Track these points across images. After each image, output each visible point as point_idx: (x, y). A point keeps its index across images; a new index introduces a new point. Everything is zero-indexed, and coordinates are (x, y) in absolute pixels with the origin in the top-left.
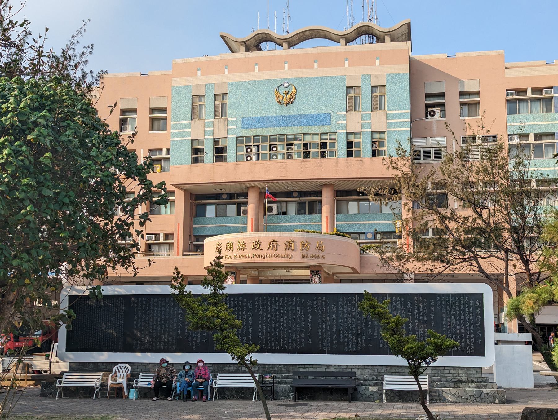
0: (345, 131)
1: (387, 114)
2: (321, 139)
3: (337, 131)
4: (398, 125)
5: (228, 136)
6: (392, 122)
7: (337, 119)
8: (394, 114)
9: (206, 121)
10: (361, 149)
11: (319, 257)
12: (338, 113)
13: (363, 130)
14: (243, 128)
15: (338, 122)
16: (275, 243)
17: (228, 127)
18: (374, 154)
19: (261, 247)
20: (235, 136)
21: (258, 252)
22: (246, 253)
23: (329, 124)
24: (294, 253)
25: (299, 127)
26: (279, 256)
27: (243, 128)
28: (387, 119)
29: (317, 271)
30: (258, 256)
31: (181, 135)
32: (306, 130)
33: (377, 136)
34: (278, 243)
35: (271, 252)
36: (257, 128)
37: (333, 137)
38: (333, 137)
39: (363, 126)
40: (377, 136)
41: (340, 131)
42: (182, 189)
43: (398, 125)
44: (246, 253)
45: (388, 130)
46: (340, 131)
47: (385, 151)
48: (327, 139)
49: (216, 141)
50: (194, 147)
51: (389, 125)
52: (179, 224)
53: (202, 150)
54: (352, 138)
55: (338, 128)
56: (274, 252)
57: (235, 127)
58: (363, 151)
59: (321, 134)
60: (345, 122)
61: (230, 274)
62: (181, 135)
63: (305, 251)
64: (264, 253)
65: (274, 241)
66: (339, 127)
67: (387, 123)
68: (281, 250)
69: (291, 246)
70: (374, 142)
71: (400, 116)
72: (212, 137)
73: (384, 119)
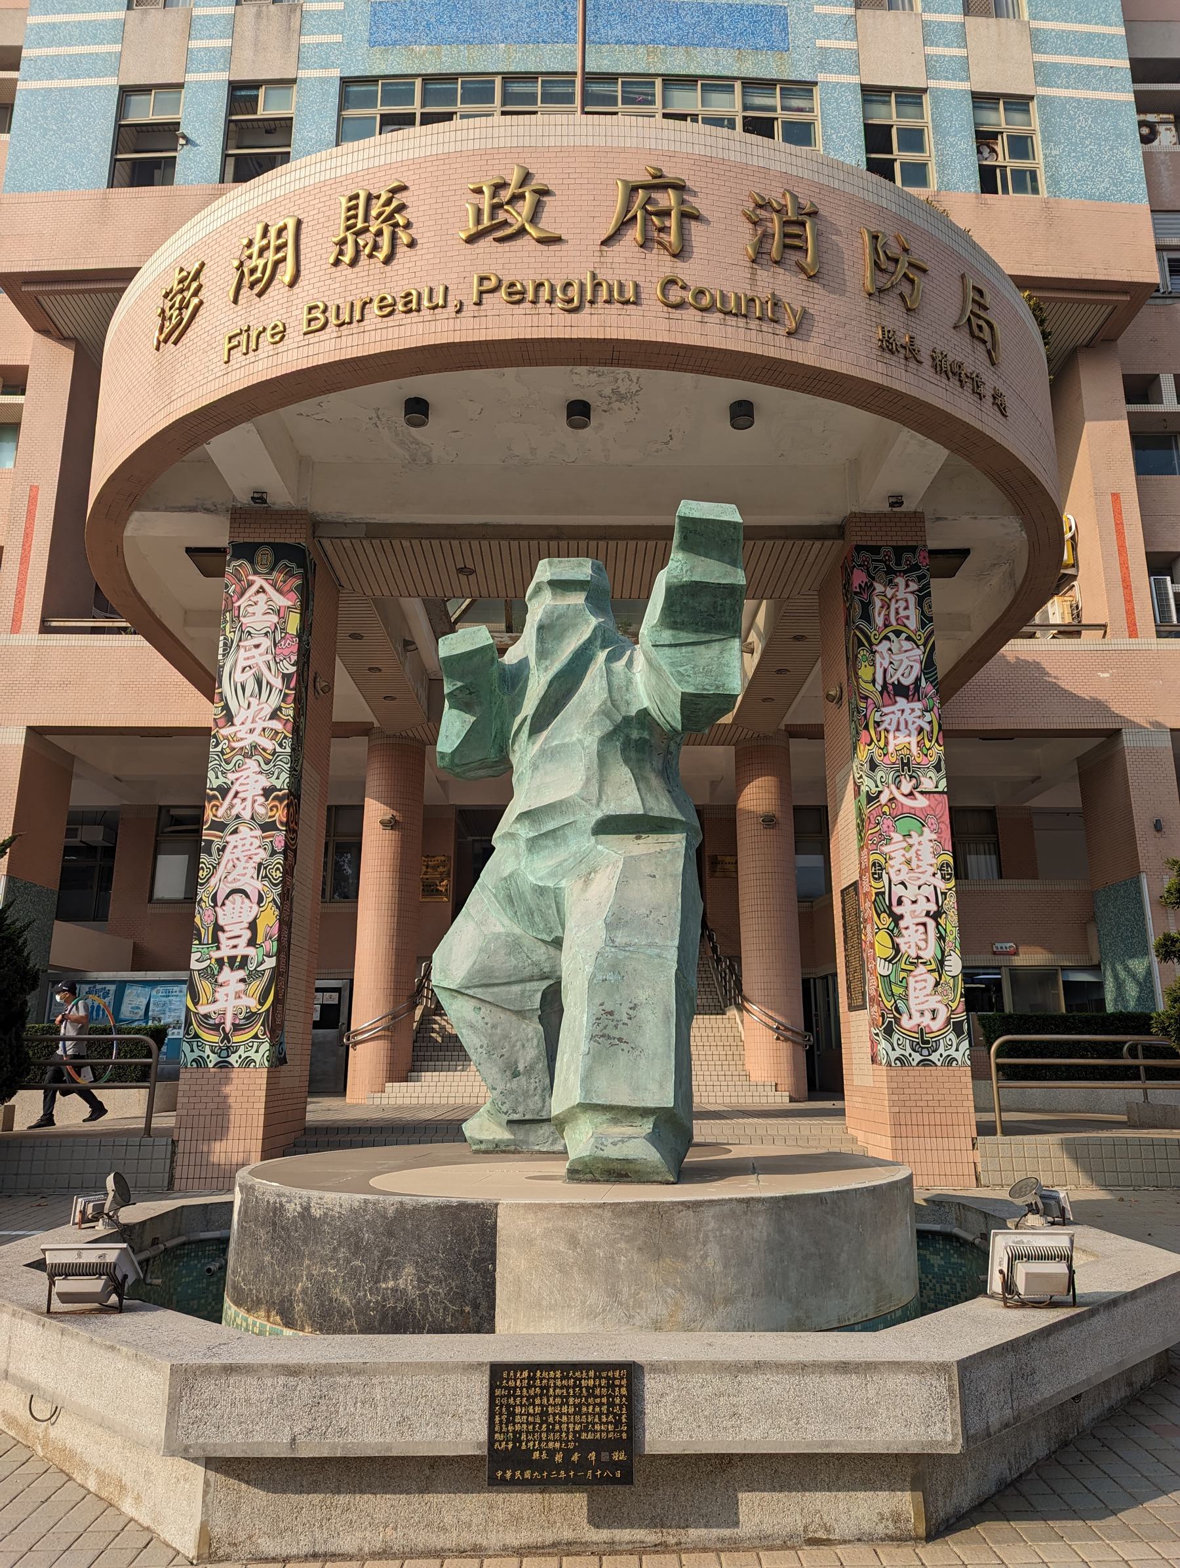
0: (855, 80)
1: (1034, 34)
2: (746, 108)
3: (821, 77)
4: (1084, 76)
5: (302, 74)
6: (1054, 65)
7: (816, 32)
8: (1060, 35)
9: (197, 12)
10: (931, 154)
11: (976, 386)
12: (818, 9)
13: (932, 84)
14: (373, 44)
15: (820, 43)
16: (667, 199)
17: (305, 40)
18: (988, 181)
19: (549, 223)
20: (336, 73)
21: (521, 262)
22: (408, 274)
23: (781, 48)
24: (819, 301)
25: (642, 49)
26: (704, 303)
27: (373, 44)
28: (1035, 50)
29: (899, 551)
30: (516, 296)
31: (74, 66)
32: (678, 64)
33: (998, 119)
34: (698, 203)
35: (629, 263)
36: (442, 41)
37: (796, 103)
38: (796, 103)
39: (931, 66)
40: (998, 119)
41: (833, 78)
42: (62, 339)
43: (1084, 76)
44: (408, 274)
45: (1042, 91)
46: (833, 78)
47: (1033, 174)
48: (774, 109)
49: (241, 94)
50: (132, 119)
51: (1043, 73)
52: (34, 490)
53: (168, 133)
54: (890, 115)
55: (822, 67)
56: (660, 265)
57: (338, 38)
58: (942, 166)
59: (751, 84)
60: (853, 45)
61: (265, 556)
62: (74, 66)
63: (892, 301)
64: (575, 263)
65: (659, 183)
66: (825, 59)
67: (1038, 67)
68: (720, 257)
69: (792, 243)
70: (985, 138)
71: (1087, 43)
72: (224, 76)
73: (1020, 48)
